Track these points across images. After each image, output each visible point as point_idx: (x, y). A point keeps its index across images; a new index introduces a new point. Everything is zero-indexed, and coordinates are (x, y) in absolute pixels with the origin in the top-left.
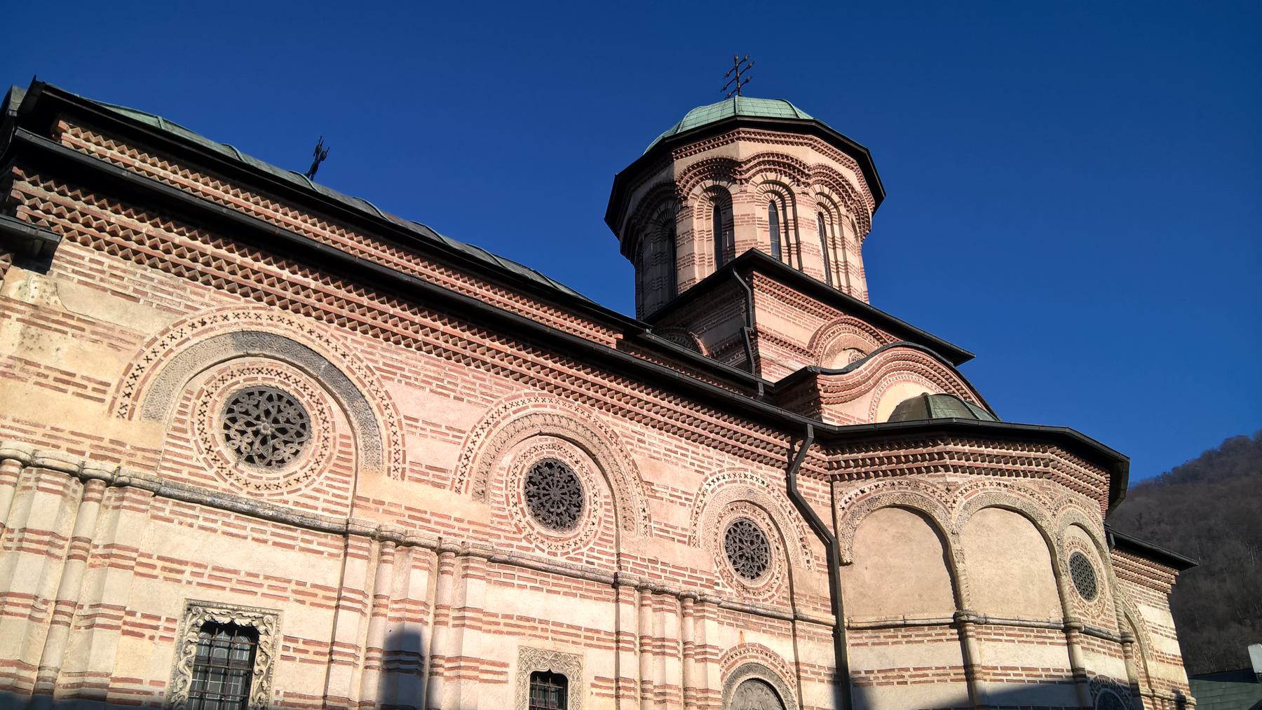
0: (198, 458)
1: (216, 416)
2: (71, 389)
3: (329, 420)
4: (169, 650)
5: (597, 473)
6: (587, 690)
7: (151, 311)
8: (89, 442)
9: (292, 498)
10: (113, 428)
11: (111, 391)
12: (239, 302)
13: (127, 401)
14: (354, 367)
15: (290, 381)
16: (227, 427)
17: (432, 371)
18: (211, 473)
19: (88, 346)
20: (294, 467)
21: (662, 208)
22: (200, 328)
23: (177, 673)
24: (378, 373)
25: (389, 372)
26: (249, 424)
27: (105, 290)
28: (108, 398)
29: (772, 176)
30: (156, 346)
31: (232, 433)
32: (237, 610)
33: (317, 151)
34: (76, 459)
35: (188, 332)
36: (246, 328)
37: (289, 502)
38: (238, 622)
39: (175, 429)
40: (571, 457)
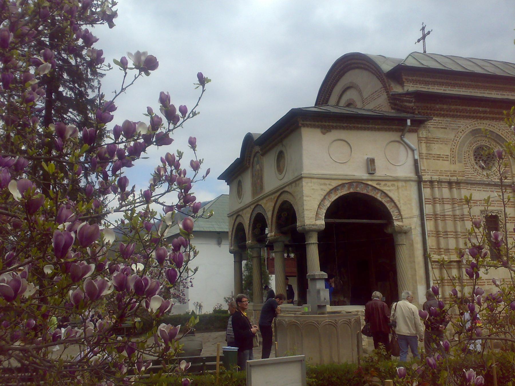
0: (471, 171)
1: (472, 157)
2: (441, 159)
8: (449, 172)
10: (453, 167)
11: (449, 157)
13: (453, 159)
14: (503, 133)
16: (475, 160)
18: (476, 174)
19: (441, 146)
22: (463, 132)
24: (510, 133)
26: (480, 158)
27: (439, 128)
28: (449, 159)
30: (455, 141)
31: (477, 161)
32: (492, 211)
33: (423, 29)
35: (461, 134)
36: (474, 129)
38: (493, 214)
39: (465, 164)
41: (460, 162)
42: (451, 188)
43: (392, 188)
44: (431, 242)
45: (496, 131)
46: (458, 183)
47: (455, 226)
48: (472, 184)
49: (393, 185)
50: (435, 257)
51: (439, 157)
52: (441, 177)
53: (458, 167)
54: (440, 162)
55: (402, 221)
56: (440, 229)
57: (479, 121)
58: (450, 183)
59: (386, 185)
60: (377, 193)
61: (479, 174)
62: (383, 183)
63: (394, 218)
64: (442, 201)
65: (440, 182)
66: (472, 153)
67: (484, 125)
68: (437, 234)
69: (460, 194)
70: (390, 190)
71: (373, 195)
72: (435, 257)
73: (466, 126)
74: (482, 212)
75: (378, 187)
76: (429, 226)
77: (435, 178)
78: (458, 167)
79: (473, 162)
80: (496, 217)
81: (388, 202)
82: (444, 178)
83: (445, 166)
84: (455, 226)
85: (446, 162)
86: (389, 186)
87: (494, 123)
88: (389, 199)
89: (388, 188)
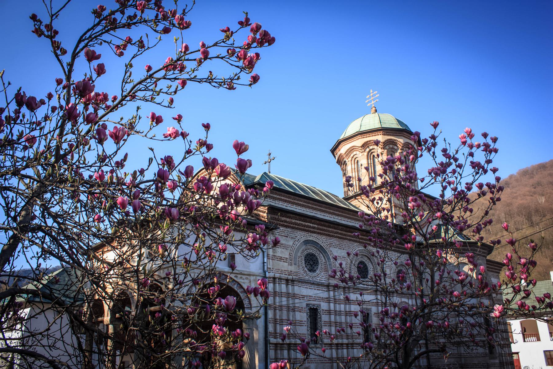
0: (302, 272)
3: (321, 259)
4: (305, 314)
5: (370, 263)
6: (373, 316)
7: (290, 239)
9: (318, 279)
12: (303, 233)
15: (313, 250)
17: (338, 243)
19: (283, 250)
20: (317, 272)
21: (355, 153)
23: (307, 319)
25: (330, 245)
29: (391, 146)
32: (314, 305)
34: (286, 276)
37: (318, 280)
40: (365, 260)
41: (295, 264)
42: (287, 285)
43: (245, 281)
44: (271, 328)
45: (320, 243)
46: (293, 281)
47: (288, 316)
48: (302, 282)
49: (247, 278)
50: (272, 340)
51: (281, 259)
52: (282, 275)
53: (293, 268)
54: (282, 263)
55: (251, 309)
56: (278, 317)
57: (310, 234)
58: (287, 280)
59: (241, 278)
60: (235, 284)
61: (307, 275)
62: (239, 276)
63: (245, 306)
64: (281, 295)
65: (280, 279)
66: (303, 258)
67: (313, 237)
68: (275, 321)
69: (293, 289)
70: (244, 283)
71: (231, 286)
72: (272, 340)
73: (302, 236)
74: (307, 305)
75: (235, 279)
76: (270, 314)
77: (277, 275)
78: (293, 268)
79: (304, 265)
80: (316, 309)
81: (241, 292)
82: (284, 276)
83: (285, 266)
84: (288, 316)
85: (286, 263)
86: (243, 279)
87: (319, 236)
88: (242, 290)
89: (243, 281)
